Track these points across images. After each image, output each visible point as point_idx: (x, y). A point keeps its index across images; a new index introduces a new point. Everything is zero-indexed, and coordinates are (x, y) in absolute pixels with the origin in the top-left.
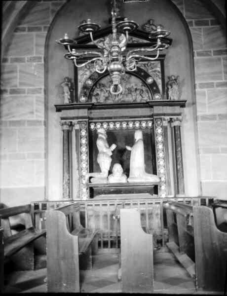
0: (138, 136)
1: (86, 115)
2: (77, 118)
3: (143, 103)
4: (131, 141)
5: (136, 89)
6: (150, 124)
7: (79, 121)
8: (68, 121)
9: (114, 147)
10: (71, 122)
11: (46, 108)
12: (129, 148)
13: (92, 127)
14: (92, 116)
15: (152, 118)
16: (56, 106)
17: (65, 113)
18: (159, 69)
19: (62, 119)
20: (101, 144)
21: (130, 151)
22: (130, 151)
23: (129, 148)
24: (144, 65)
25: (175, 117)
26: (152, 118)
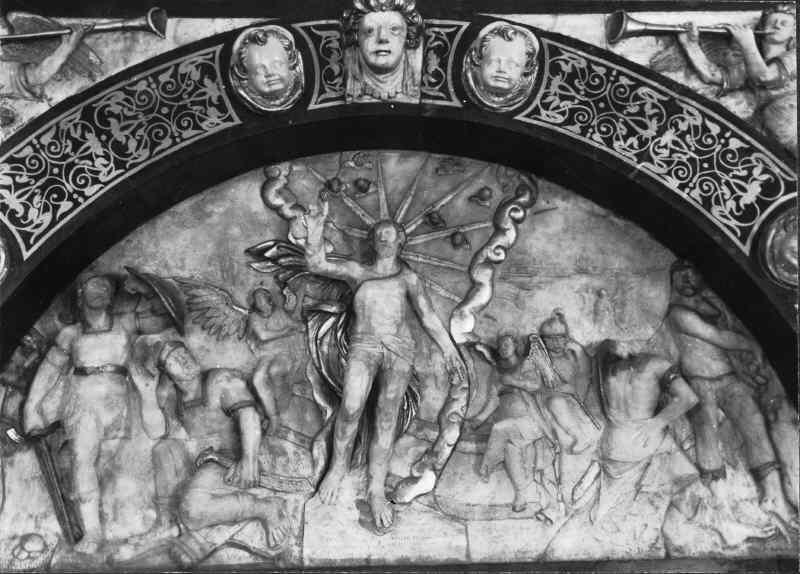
5: (605, 361)
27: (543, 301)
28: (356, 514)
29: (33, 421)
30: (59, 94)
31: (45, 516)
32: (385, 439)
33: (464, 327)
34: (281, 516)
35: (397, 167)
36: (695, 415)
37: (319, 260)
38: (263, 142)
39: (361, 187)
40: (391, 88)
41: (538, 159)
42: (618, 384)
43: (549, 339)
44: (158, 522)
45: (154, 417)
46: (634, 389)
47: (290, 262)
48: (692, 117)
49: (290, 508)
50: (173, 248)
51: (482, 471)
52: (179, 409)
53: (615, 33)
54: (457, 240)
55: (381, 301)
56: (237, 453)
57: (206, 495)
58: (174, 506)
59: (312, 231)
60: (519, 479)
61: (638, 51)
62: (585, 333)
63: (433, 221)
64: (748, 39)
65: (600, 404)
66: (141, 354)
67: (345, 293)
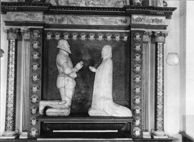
0: (107, 52)
1: (41, 20)
2: (26, 24)
3: (120, 9)
4: (97, 60)
6: (126, 38)
7: (31, 29)
8: (14, 27)
9: (79, 66)
10: (20, 29)
12: (93, 69)
13: (49, 37)
14: (47, 22)
15: (128, 31)
17: (13, 17)
20: (63, 60)
21: (95, 73)
22: (95, 73)
23: (93, 69)
25: (158, 31)
26: (128, 31)
28: (85, 4)
31: (55, 3)
34: (78, 4)
44: (66, 4)
49: (78, 3)
60: (101, 2)
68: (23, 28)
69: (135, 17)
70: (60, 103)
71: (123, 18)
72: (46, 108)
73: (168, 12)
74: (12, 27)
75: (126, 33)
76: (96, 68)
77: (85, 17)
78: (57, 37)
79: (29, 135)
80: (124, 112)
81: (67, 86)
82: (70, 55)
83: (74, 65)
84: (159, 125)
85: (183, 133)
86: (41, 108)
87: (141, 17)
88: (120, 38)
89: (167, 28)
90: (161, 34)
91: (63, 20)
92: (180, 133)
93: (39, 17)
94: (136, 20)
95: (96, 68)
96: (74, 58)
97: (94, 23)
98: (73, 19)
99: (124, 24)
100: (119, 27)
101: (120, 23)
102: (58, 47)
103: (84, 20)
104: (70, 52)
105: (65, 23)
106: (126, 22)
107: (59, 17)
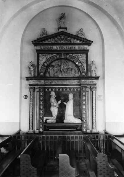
0: (71, 96)
1: (43, 83)
2: (37, 85)
3: (76, 77)
4: (67, 100)
5: (72, 69)
6: (79, 89)
8: (33, 87)
9: (59, 102)
10: (35, 87)
11: (21, 78)
15: (80, 86)
16: (26, 77)
17: (32, 82)
18: (85, 58)
19: (30, 85)
20: (53, 100)
22: (65, 105)
23: (65, 103)
24: (77, 55)
25: (92, 87)
27: (69, 66)
29: (48, 71)
30: (49, 57)
32: (62, 72)
33: (66, 67)
35: (63, 60)
36: (75, 71)
37: (60, 64)
38: (57, 59)
39: (62, 61)
40: (63, 57)
41: (69, 60)
42: (72, 70)
43: (70, 68)
45: (53, 71)
46: (73, 70)
47: (58, 64)
48: (76, 59)
50: (53, 64)
51: (67, 73)
52: (54, 71)
53: (73, 55)
54: (66, 64)
55: (62, 66)
56: (56, 73)
57: (55, 74)
58: (54, 75)
59: (59, 63)
61: (73, 56)
62: (71, 68)
63: (65, 63)
64: (78, 56)
65: (72, 71)
66: (52, 69)
67: (61, 66)
68: (36, 87)
69: (83, 81)
70: (52, 117)
71: (78, 81)
72: (47, 119)
73: (97, 78)
74: (31, 86)
75: (79, 87)
76: (67, 103)
77: (61, 81)
78: (50, 90)
79: (39, 131)
80: (78, 121)
81: (55, 111)
82: (55, 98)
83: (57, 102)
84: (94, 127)
85: (105, 130)
86: (44, 120)
87: (85, 80)
88: (77, 89)
89: (97, 85)
90: (94, 88)
91: (52, 82)
92: (104, 130)
93: (42, 82)
94: (83, 82)
95: (67, 103)
96: (57, 99)
97: (65, 83)
98: (56, 82)
99: (78, 83)
100: (76, 85)
101: (76, 83)
102: (51, 94)
103: (61, 82)
104: (56, 96)
105: (53, 83)
106: (79, 82)
107: (50, 81)
